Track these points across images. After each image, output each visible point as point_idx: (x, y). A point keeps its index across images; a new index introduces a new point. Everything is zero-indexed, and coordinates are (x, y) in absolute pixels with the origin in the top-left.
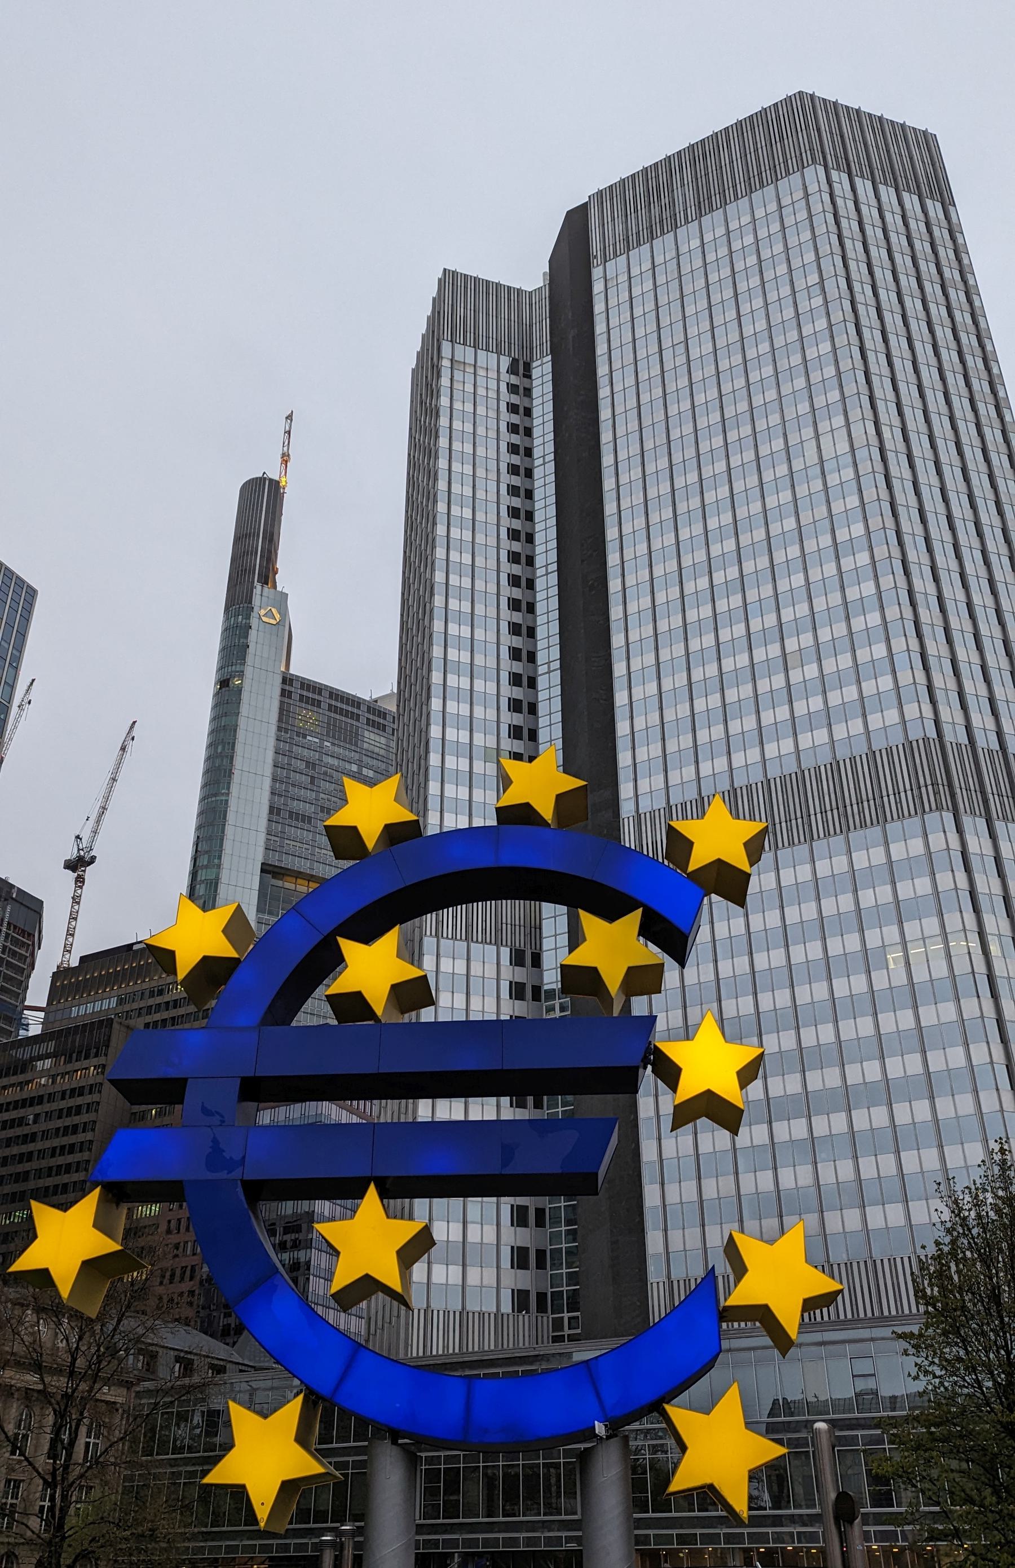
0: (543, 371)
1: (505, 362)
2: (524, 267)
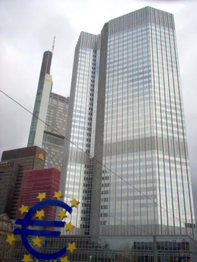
0: (98, 52)
1: (92, 50)
2: (97, 31)
